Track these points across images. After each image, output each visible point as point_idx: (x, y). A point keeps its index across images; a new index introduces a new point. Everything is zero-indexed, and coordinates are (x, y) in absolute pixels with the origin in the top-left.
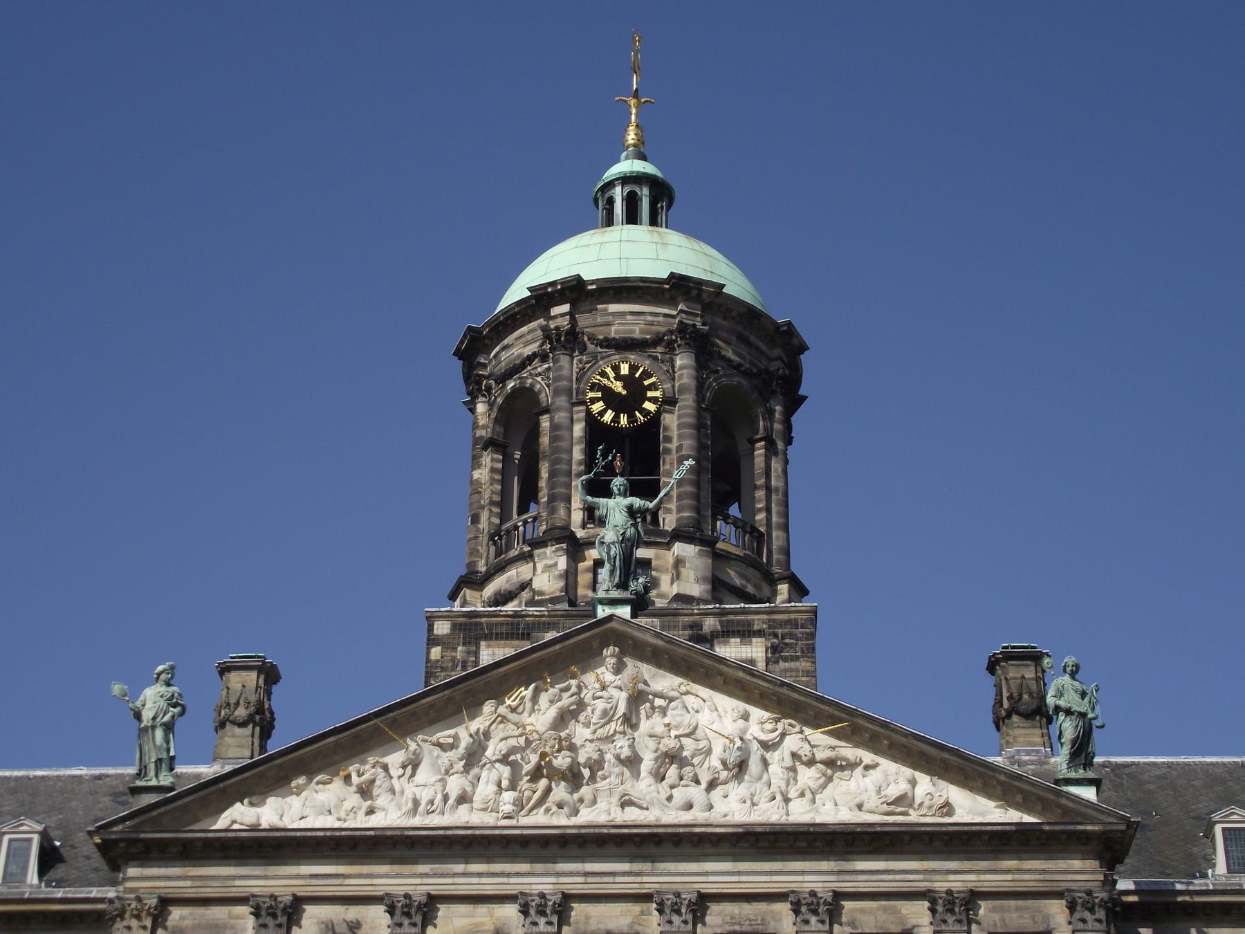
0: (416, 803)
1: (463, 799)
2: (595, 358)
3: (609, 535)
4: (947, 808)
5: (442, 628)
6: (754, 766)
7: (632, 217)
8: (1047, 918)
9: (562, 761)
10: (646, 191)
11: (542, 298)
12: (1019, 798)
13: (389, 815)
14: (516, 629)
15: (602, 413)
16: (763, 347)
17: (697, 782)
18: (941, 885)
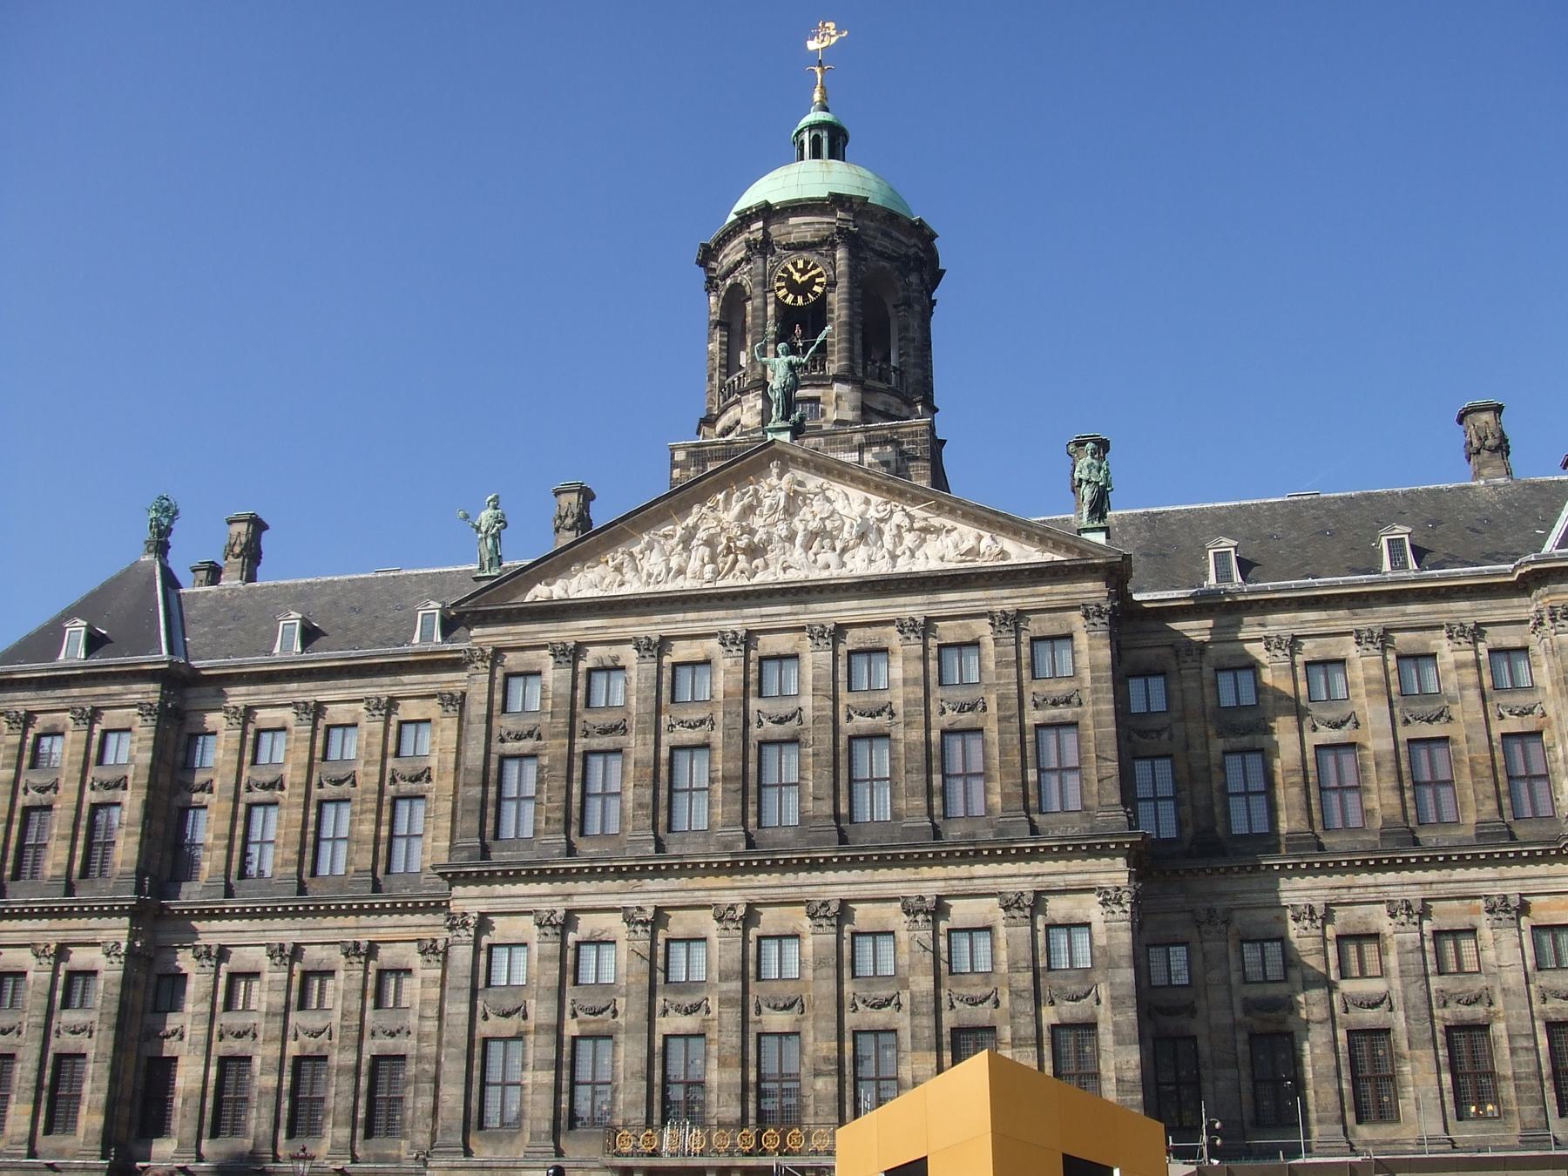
0: (650, 575)
1: (681, 571)
2: (781, 258)
4: (1003, 554)
5: (680, 456)
6: (872, 537)
7: (816, 154)
8: (1069, 625)
9: (742, 543)
10: (825, 134)
12: (1050, 543)
13: (634, 587)
14: (728, 451)
15: (785, 297)
16: (903, 239)
17: (834, 549)
18: (997, 608)
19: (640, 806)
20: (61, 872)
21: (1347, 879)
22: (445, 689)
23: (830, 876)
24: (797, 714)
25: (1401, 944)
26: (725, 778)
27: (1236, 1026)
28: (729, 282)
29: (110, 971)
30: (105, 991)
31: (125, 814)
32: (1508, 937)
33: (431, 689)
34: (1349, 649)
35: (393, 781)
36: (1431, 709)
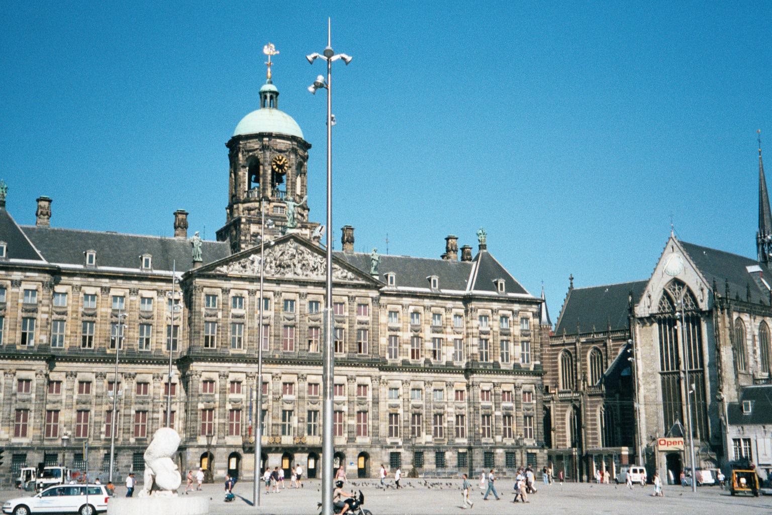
3: (290, 212)
11: (260, 136)
13: (249, 273)
19: (251, 342)
20: (11, 342)
21: (415, 374)
22: (160, 289)
23: (305, 367)
24: (294, 319)
25: (426, 393)
26: (275, 336)
27: (387, 411)
28: (251, 154)
29: (37, 381)
30: (37, 388)
31: (39, 323)
32: (450, 392)
33: (154, 287)
34: (421, 309)
35: (140, 318)
36: (439, 329)
